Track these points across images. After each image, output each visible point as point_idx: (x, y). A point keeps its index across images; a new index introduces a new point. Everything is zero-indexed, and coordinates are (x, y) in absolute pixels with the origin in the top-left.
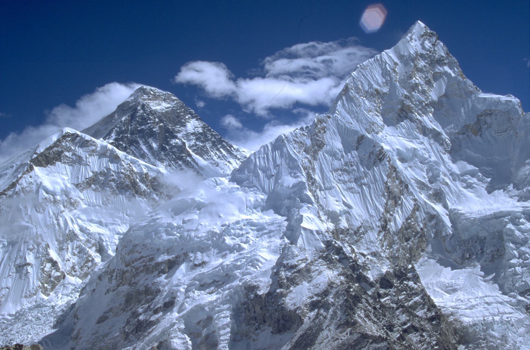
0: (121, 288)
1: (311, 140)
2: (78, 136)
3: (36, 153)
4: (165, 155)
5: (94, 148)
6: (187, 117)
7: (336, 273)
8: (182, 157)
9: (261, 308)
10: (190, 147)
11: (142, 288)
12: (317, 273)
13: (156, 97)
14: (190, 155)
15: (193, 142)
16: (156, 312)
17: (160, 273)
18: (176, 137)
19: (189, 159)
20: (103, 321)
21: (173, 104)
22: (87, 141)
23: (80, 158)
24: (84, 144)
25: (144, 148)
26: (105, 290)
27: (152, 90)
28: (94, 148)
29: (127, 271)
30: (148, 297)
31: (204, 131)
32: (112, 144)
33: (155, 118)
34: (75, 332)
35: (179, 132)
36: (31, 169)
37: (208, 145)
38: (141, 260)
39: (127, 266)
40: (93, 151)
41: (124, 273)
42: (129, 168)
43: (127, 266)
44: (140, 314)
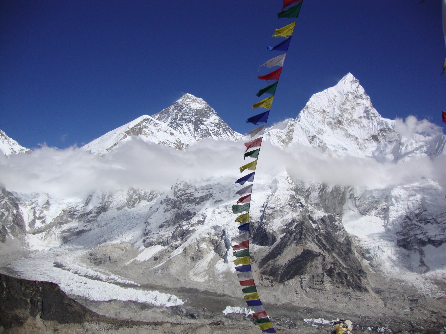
4: (197, 134)
5: (160, 127)
7: (297, 214)
12: (286, 213)
13: (194, 101)
15: (212, 128)
16: (193, 225)
17: (196, 203)
23: (152, 132)
24: (156, 124)
28: (160, 127)
29: (178, 201)
37: (221, 130)
38: (186, 196)
39: (177, 198)
40: (160, 129)
41: (176, 202)
43: (177, 198)
44: (184, 226)
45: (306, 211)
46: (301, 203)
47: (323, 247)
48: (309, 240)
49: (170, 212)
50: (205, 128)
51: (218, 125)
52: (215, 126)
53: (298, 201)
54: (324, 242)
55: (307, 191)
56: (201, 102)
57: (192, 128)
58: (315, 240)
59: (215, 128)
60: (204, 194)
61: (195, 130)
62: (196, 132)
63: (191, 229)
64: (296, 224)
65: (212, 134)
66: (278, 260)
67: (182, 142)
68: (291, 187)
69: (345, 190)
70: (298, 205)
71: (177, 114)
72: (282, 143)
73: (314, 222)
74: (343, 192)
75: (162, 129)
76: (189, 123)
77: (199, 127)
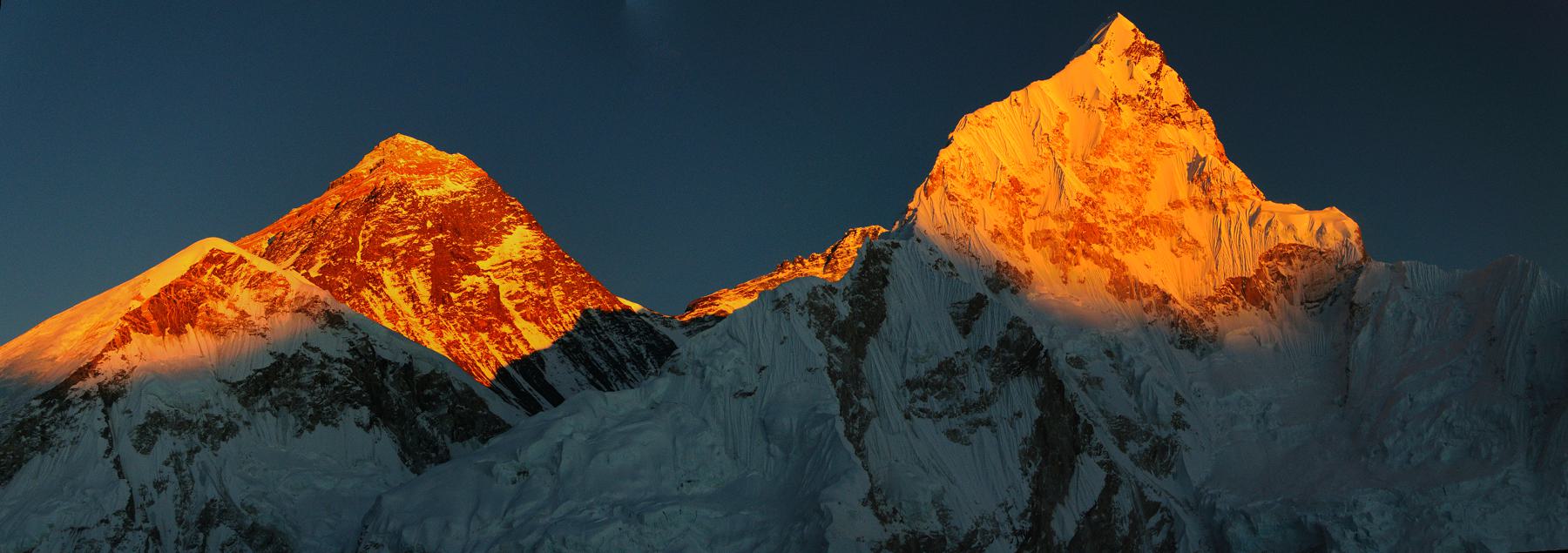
1: (851, 303)
2: (241, 260)
3: (138, 298)
4: (448, 317)
5: (280, 292)
6: (504, 220)
8: (490, 322)
10: (510, 298)
13: (425, 168)
14: (511, 322)
15: (515, 287)
18: (477, 271)
19: (506, 329)
21: (473, 183)
22: (262, 274)
23: (243, 314)
25: (393, 291)
27: (418, 147)
31: (546, 258)
33: (425, 221)
35: (484, 256)
36: (125, 338)
37: (557, 293)
42: (365, 348)
50: (485, 288)
51: (541, 271)
52: (526, 278)
56: (458, 168)
57: (424, 291)
59: (530, 286)
61: (438, 297)
62: (441, 309)
65: (516, 315)
68: (887, 536)
71: (352, 229)
72: (836, 342)
75: (290, 296)
76: (408, 269)
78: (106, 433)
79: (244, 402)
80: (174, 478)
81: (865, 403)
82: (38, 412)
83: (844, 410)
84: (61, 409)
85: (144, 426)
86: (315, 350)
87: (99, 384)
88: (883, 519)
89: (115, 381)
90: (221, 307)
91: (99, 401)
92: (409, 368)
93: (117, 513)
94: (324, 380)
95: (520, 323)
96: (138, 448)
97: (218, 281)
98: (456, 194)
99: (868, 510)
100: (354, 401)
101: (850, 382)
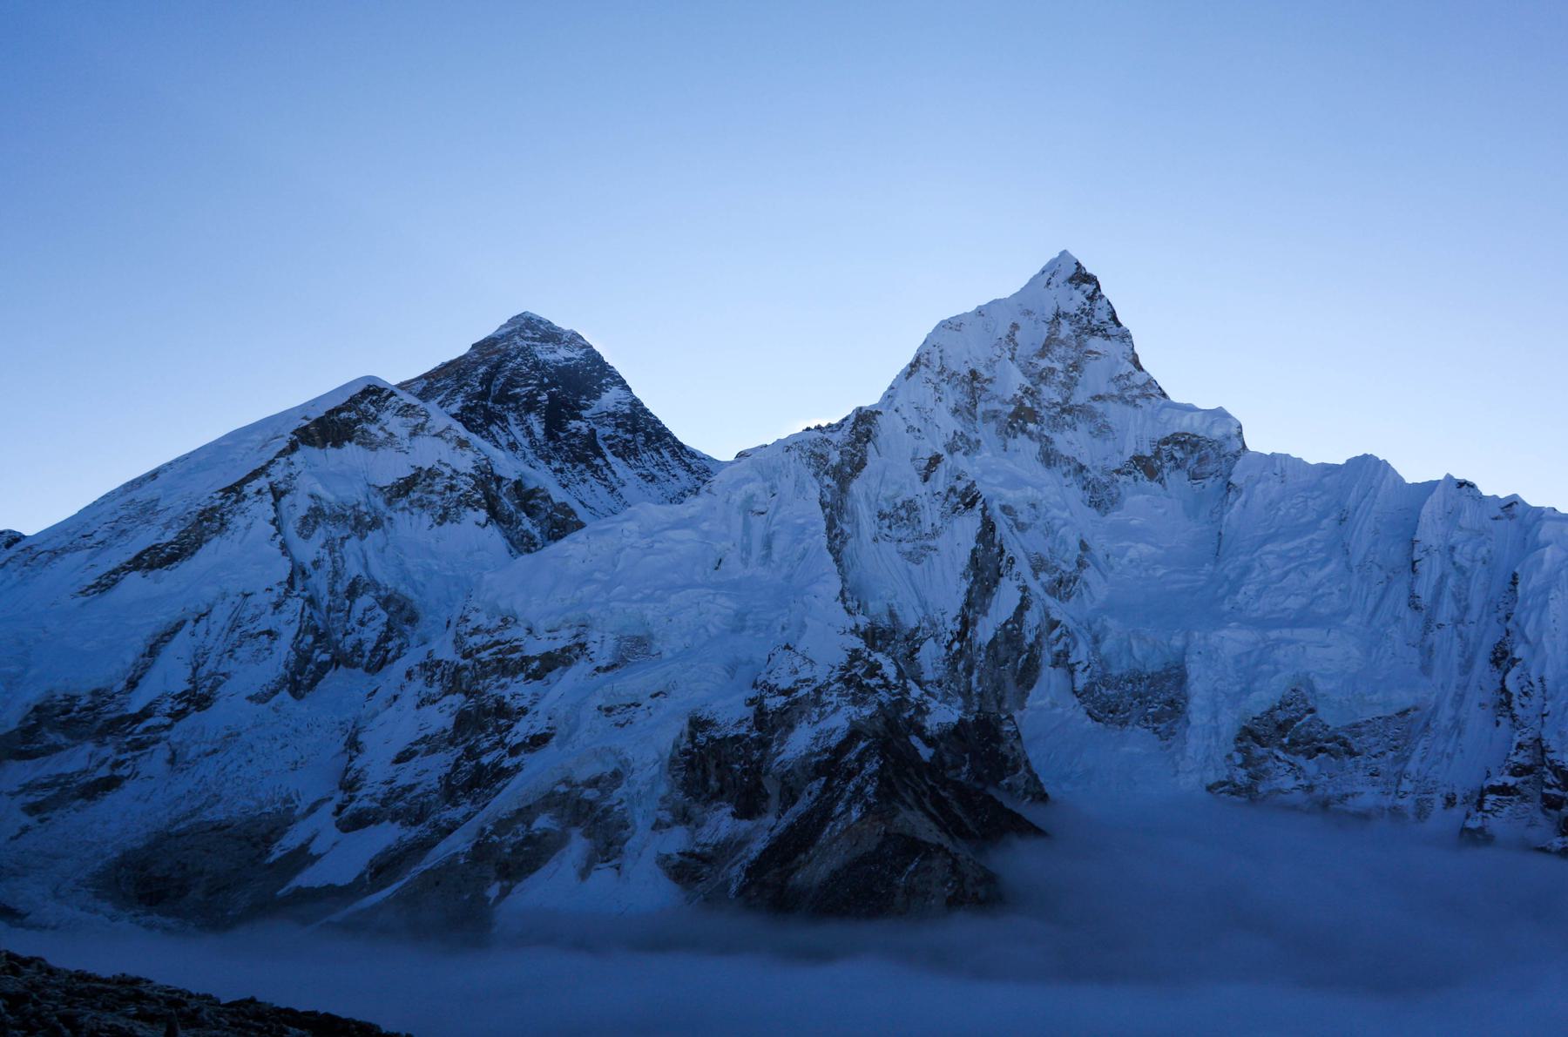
0: (448, 699)
4: (555, 450)
5: (422, 420)
9: (718, 766)
11: (491, 704)
14: (603, 457)
15: (608, 431)
16: (514, 751)
17: (528, 676)
18: (579, 418)
19: (599, 461)
20: (408, 759)
22: (408, 406)
26: (418, 700)
29: (465, 668)
30: (502, 721)
32: (454, 416)
34: (351, 774)
35: (586, 407)
38: (495, 649)
39: (464, 657)
41: (459, 670)
44: (483, 753)
45: (901, 704)
46: (882, 677)
47: (955, 828)
48: (903, 802)
49: (437, 706)
50: (585, 430)
52: (617, 426)
53: (873, 670)
54: (957, 810)
55: (907, 639)
57: (538, 429)
58: (926, 800)
59: (620, 432)
60: (560, 644)
61: (550, 434)
62: (551, 444)
63: (508, 763)
64: (862, 745)
66: (792, 872)
67: (497, 472)
69: (1037, 637)
70: (873, 682)
72: (828, 480)
73: (929, 742)
74: (1031, 646)
76: (528, 412)
77: (561, 428)
78: (273, 522)
79: (389, 502)
80: (327, 558)
81: (845, 527)
82: (218, 503)
83: (829, 529)
84: (236, 502)
85: (305, 517)
86: (447, 465)
87: (271, 484)
88: (849, 612)
89: (285, 481)
90: (373, 429)
91: (270, 496)
92: (518, 485)
93: (280, 584)
94: (452, 488)
95: (610, 458)
96: (300, 534)
97: (372, 409)
98: (567, 360)
99: (839, 604)
100: (475, 505)
101: (835, 510)
